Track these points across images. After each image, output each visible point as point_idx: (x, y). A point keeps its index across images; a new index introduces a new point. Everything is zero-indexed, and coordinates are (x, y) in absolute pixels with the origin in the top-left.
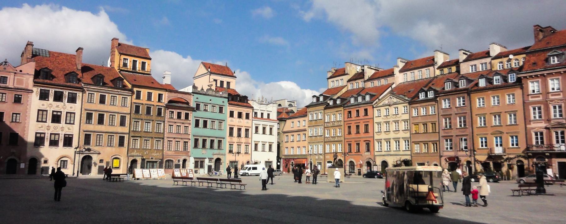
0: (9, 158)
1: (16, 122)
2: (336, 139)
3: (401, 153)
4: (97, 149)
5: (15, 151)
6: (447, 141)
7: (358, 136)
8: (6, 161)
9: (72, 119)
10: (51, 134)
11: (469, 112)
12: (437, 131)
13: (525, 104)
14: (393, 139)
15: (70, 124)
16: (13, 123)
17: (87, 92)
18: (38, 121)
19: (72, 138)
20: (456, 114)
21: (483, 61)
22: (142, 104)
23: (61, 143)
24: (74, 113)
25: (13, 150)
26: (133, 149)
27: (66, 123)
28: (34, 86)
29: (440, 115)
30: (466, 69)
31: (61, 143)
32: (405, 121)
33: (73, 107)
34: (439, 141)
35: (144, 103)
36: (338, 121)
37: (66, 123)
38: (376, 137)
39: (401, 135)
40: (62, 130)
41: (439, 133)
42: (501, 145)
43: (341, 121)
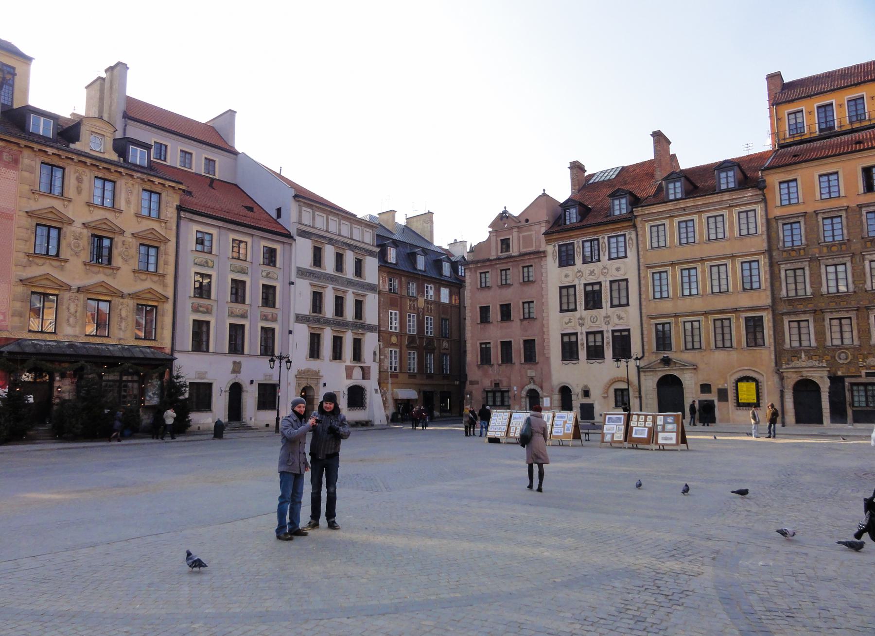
0: (528, 387)
1: (529, 318)
4: (688, 357)
5: (533, 374)
8: (524, 393)
9: (623, 294)
10: (588, 333)
15: (620, 305)
16: (525, 322)
17: (647, 226)
18: (562, 311)
19: (629, 336)
22: (805, 214)
23: (608, 352)
24: (626, 280)
25: (531, 373)
26: (795, 354)
27: (612, 306)
28: (548, 242)
31: (608, 352)
33: (622, 266)
35: (810, 210)
37: (612, 306)
40: (607, 323)
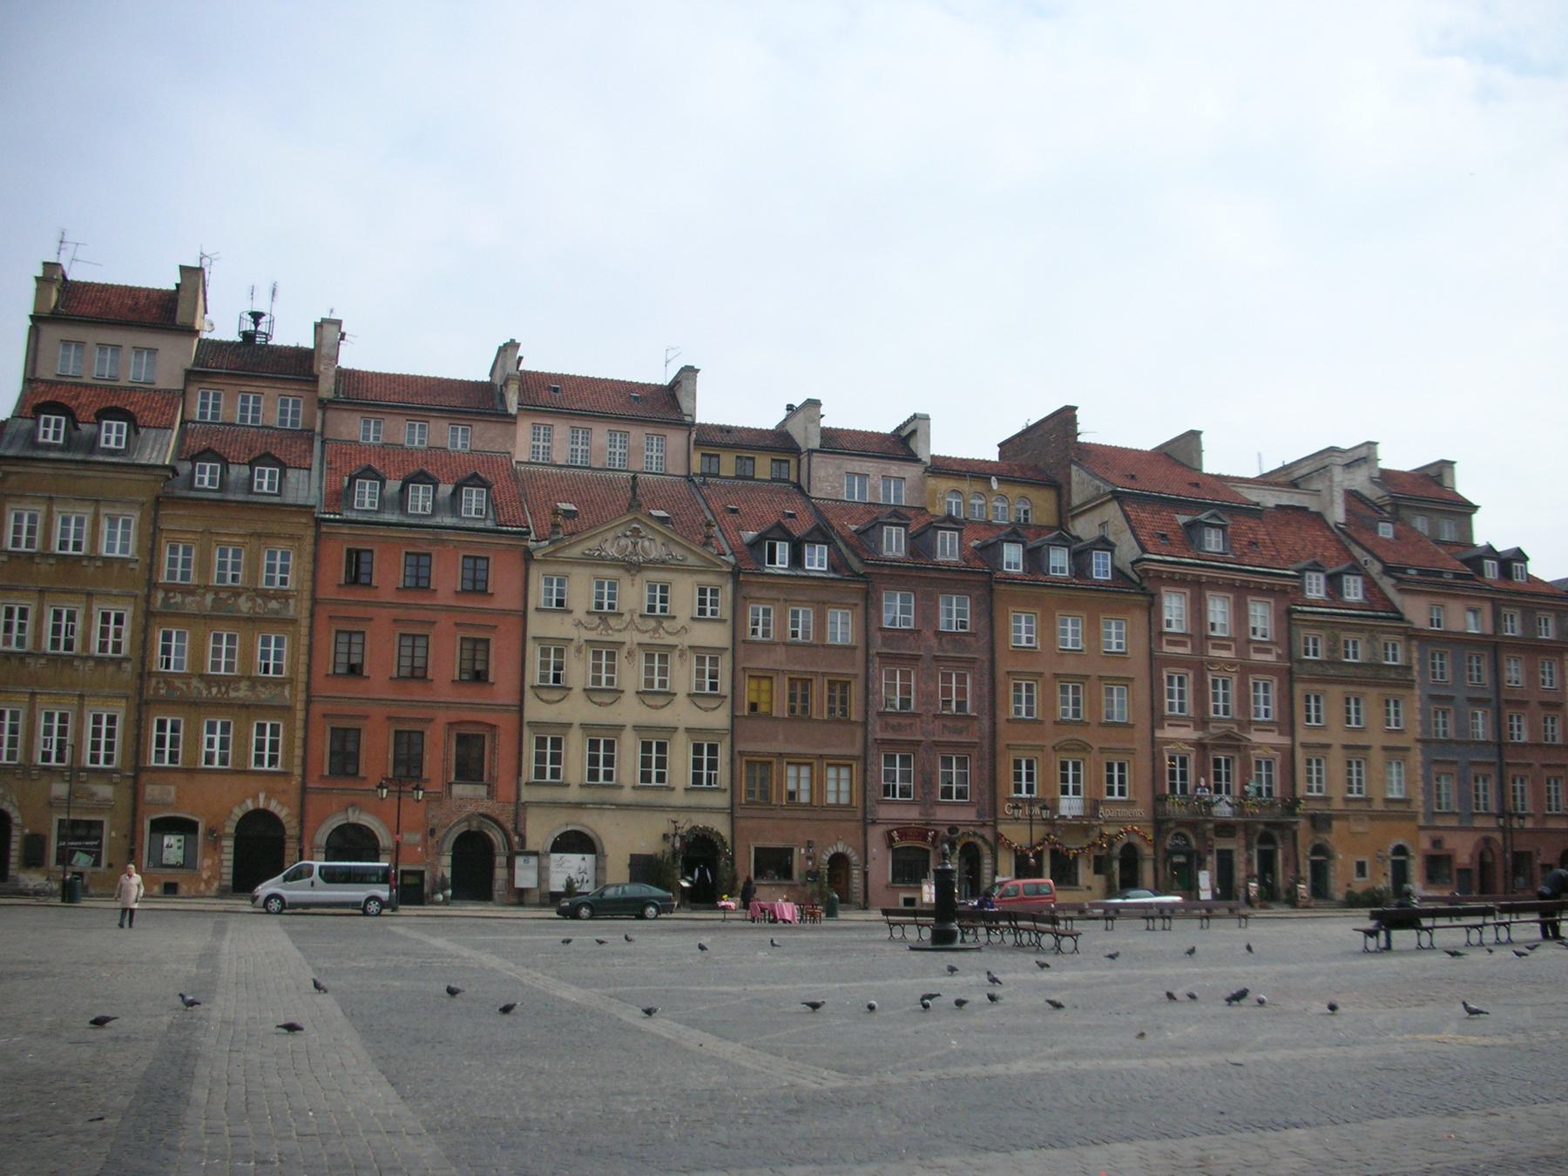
2: (242, 692)
3: (678, 798)
6: (890, 760)
7: (417, 692)
11: (985, 657)
12: (855, 714)
13: (1155, 662)
14: (637, 728)
20: (936, 658)
21: (895, 469)
29: (873, 651)
30: (829, 480)
32: (700, 652)
34: (864, 758)
36: (265, 595)
38: (535, 710)
39: (681, 714)
41: (865, 724)
42: (1076, 791)
43: (283, 596)
